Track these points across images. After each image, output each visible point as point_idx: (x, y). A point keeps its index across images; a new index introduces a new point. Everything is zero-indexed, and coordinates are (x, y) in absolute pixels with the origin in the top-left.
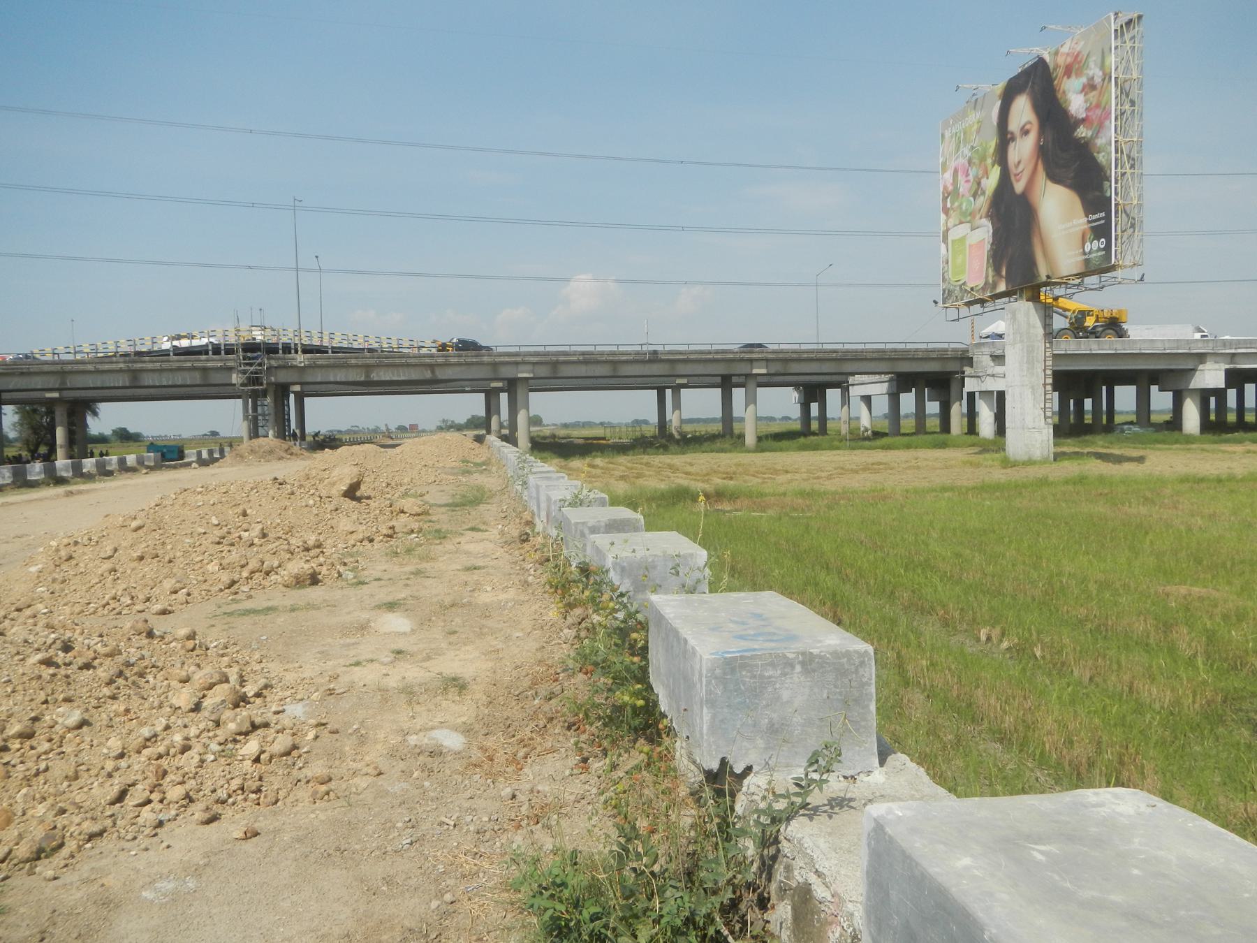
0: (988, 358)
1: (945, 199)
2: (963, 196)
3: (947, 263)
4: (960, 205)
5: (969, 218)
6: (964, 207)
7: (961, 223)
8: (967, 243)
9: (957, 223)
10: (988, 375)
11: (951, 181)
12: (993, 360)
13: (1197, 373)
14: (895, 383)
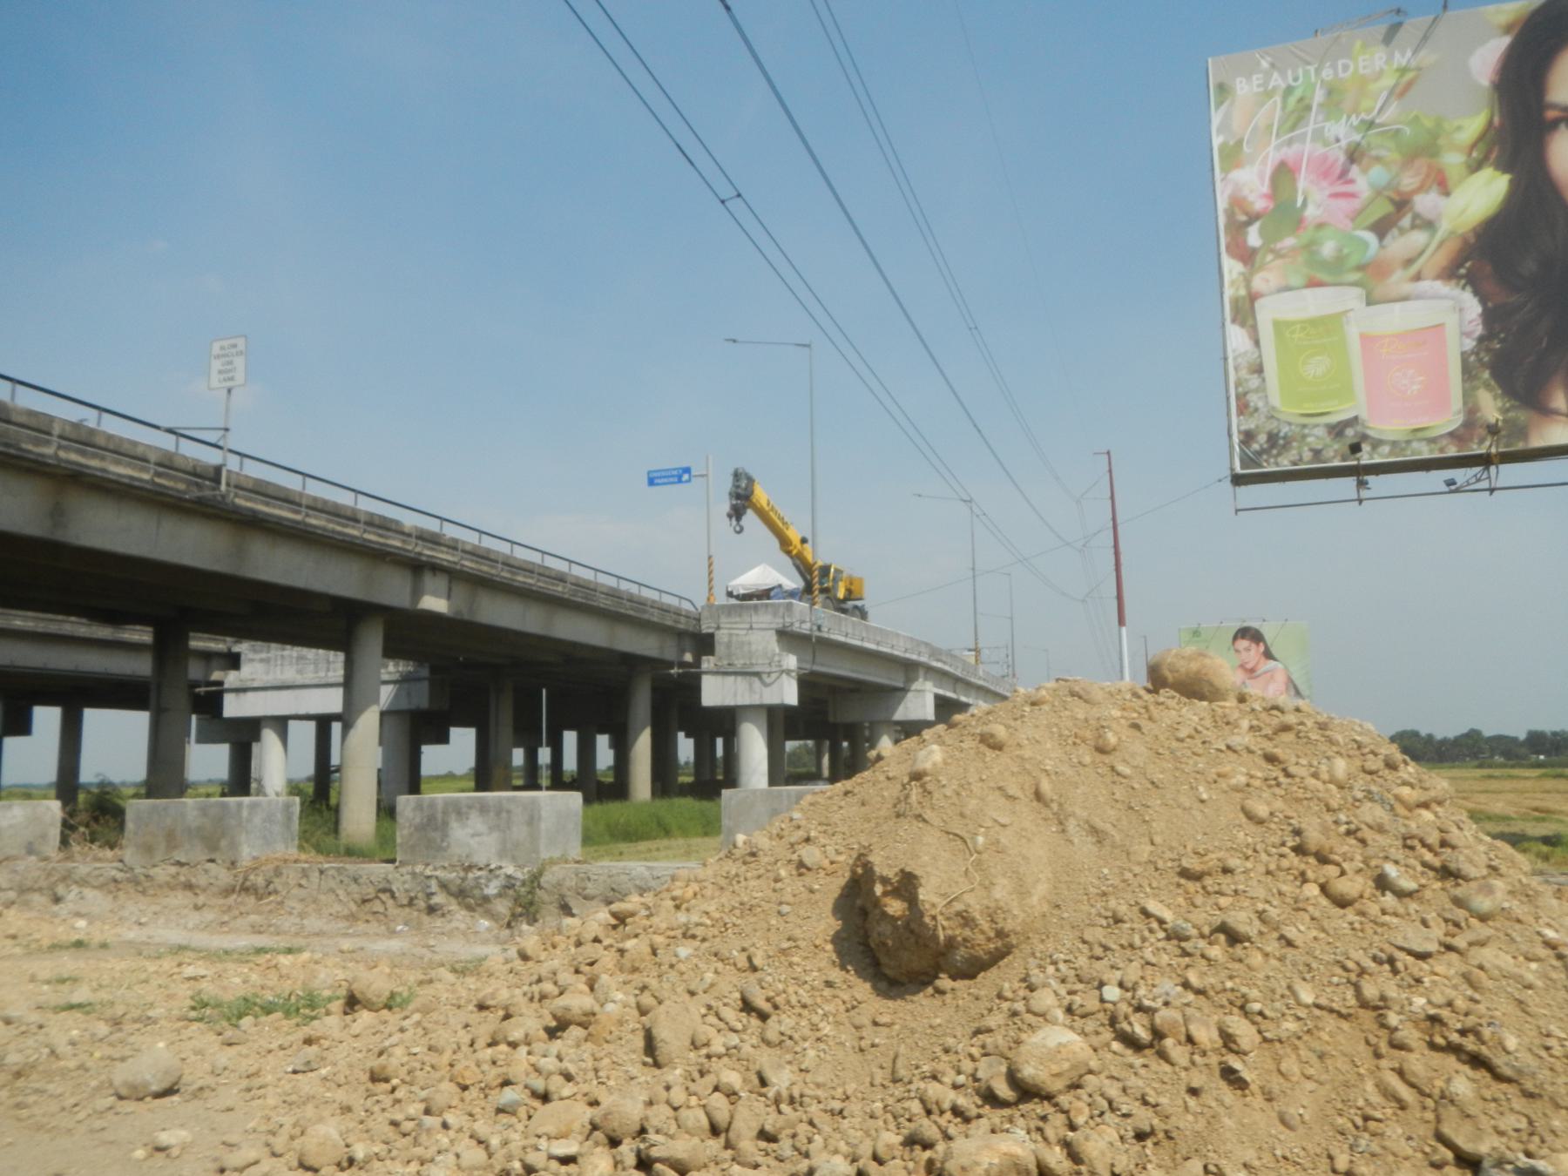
0: (772, 639)
1: (1237, 229)
2: (1320, 226)
3: (1259, 370)
4: (1310, 247)
5: (1356, 276)
6: (1328, 249)
7: (1313, 284)
8: (1353, 332)
9: (1296, 280)
10: (783, 672)
11: (1265, 189)
12: (778, 641)
13: (910, 695)
14: (425, 685)
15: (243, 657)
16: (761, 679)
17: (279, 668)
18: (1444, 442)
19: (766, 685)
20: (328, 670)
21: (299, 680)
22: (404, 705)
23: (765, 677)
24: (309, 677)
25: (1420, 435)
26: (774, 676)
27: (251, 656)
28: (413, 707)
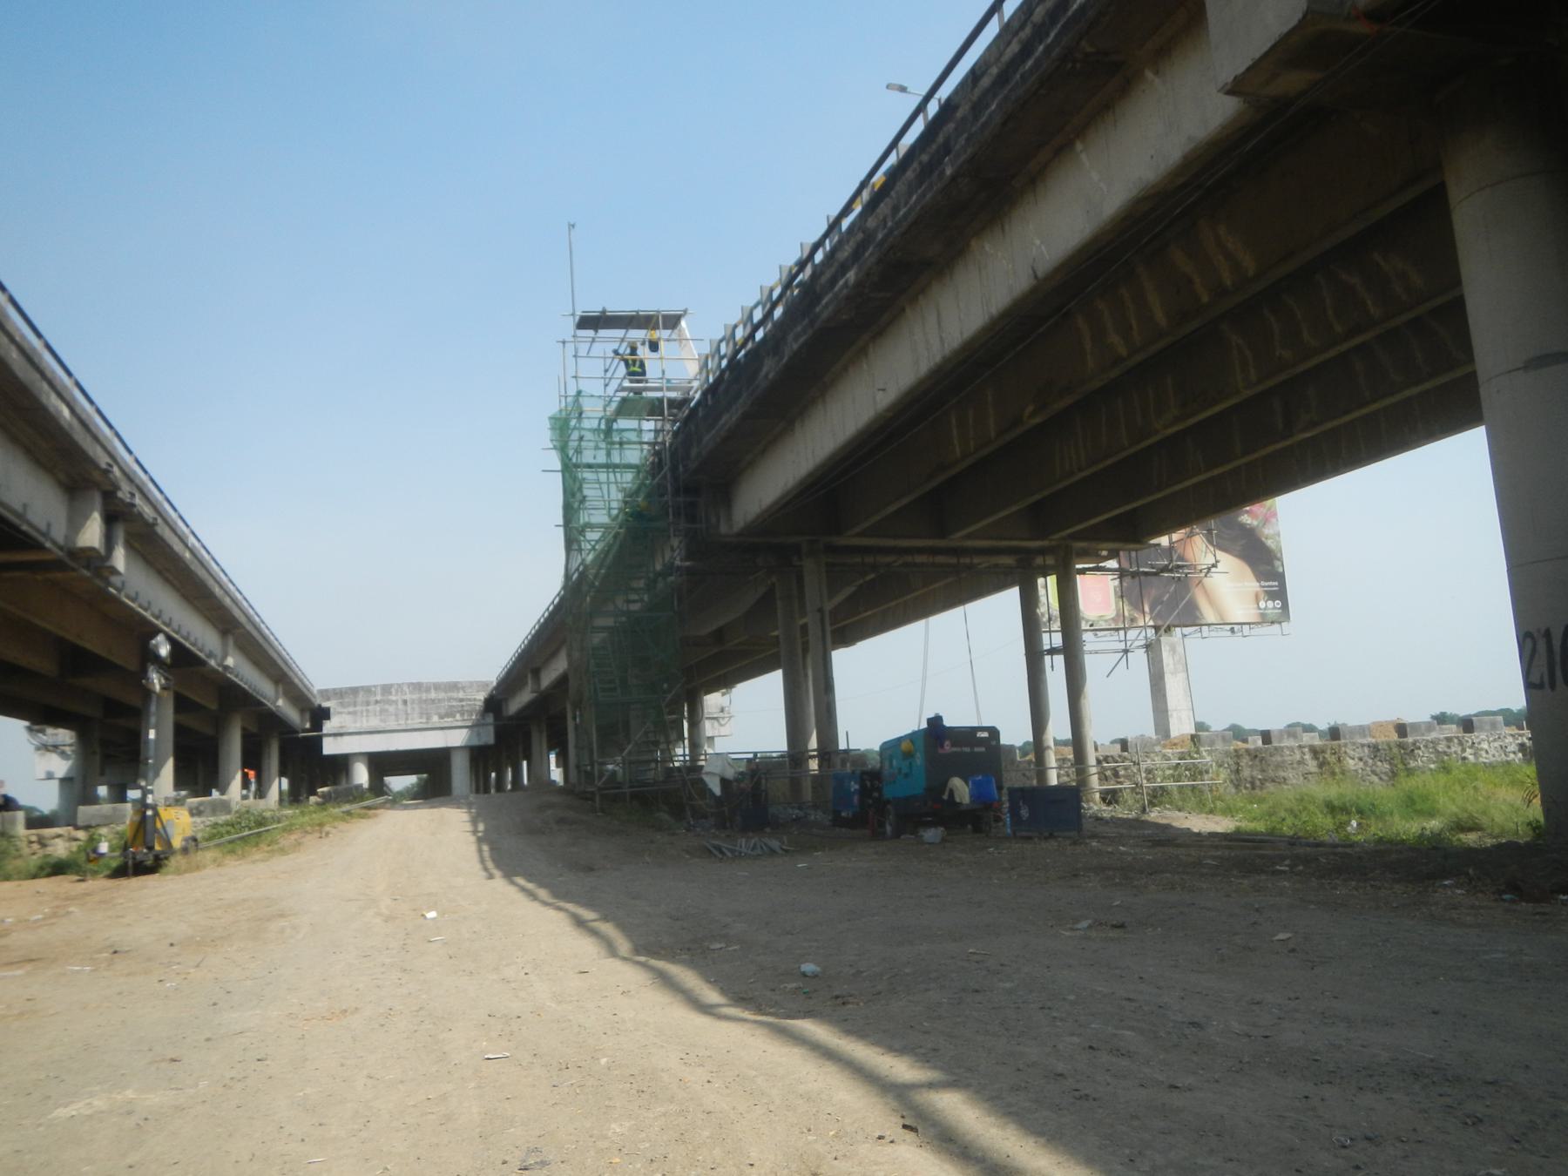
15: (332, 710)
16: (718, 721)
17: (364, 719)
18: (1111, 622)
19: (721, 725)
20: (407, 719)
21: (382, 726)
22: (476, 742)
23: (721, 720)
24: (392, 725)
26: (726, 719)
27: (340, 709)
28: (481, 743)
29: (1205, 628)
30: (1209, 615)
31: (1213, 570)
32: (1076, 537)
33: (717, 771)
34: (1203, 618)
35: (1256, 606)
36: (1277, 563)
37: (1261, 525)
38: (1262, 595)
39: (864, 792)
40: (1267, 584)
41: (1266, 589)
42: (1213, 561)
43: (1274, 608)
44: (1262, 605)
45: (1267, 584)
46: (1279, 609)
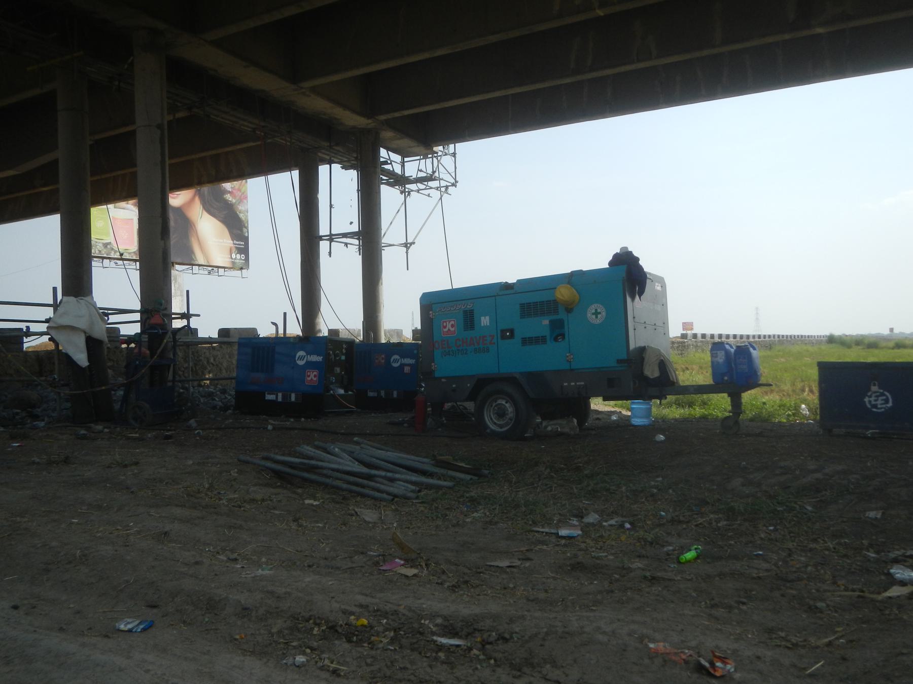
18: (133, 254)
25: (127, 251)
29: (196, 268)
30: (201, 260)
31: (451, 189)
32: (391, 125)
33: (82, 324)
34: (197, 260)
35: (230, 256)
36: (245, 230)
37: (237, 203)
38: (234, 250)
39: (325, 368)
40: (237, 243)
41: (236, 246)
42: (453, 181)
43: (241, 259)
44: (234, 256)
45: (237, 243)
46: (243, 260)
